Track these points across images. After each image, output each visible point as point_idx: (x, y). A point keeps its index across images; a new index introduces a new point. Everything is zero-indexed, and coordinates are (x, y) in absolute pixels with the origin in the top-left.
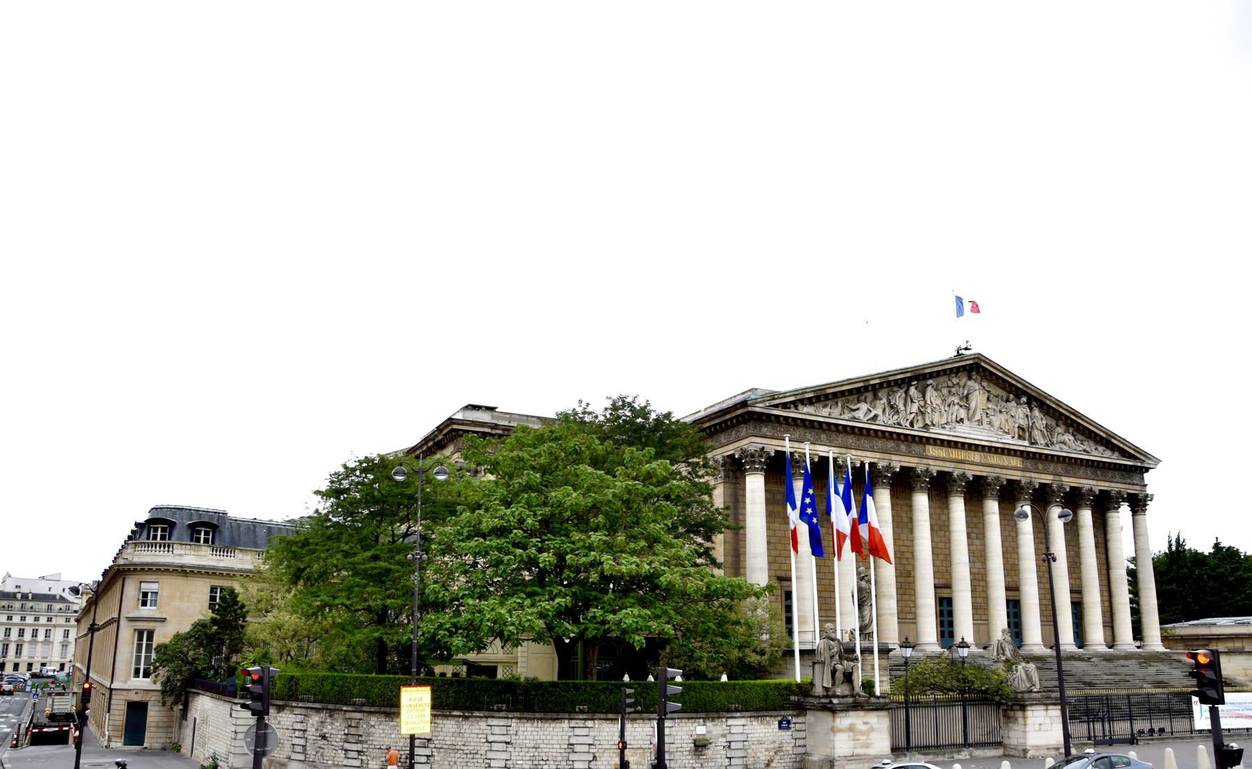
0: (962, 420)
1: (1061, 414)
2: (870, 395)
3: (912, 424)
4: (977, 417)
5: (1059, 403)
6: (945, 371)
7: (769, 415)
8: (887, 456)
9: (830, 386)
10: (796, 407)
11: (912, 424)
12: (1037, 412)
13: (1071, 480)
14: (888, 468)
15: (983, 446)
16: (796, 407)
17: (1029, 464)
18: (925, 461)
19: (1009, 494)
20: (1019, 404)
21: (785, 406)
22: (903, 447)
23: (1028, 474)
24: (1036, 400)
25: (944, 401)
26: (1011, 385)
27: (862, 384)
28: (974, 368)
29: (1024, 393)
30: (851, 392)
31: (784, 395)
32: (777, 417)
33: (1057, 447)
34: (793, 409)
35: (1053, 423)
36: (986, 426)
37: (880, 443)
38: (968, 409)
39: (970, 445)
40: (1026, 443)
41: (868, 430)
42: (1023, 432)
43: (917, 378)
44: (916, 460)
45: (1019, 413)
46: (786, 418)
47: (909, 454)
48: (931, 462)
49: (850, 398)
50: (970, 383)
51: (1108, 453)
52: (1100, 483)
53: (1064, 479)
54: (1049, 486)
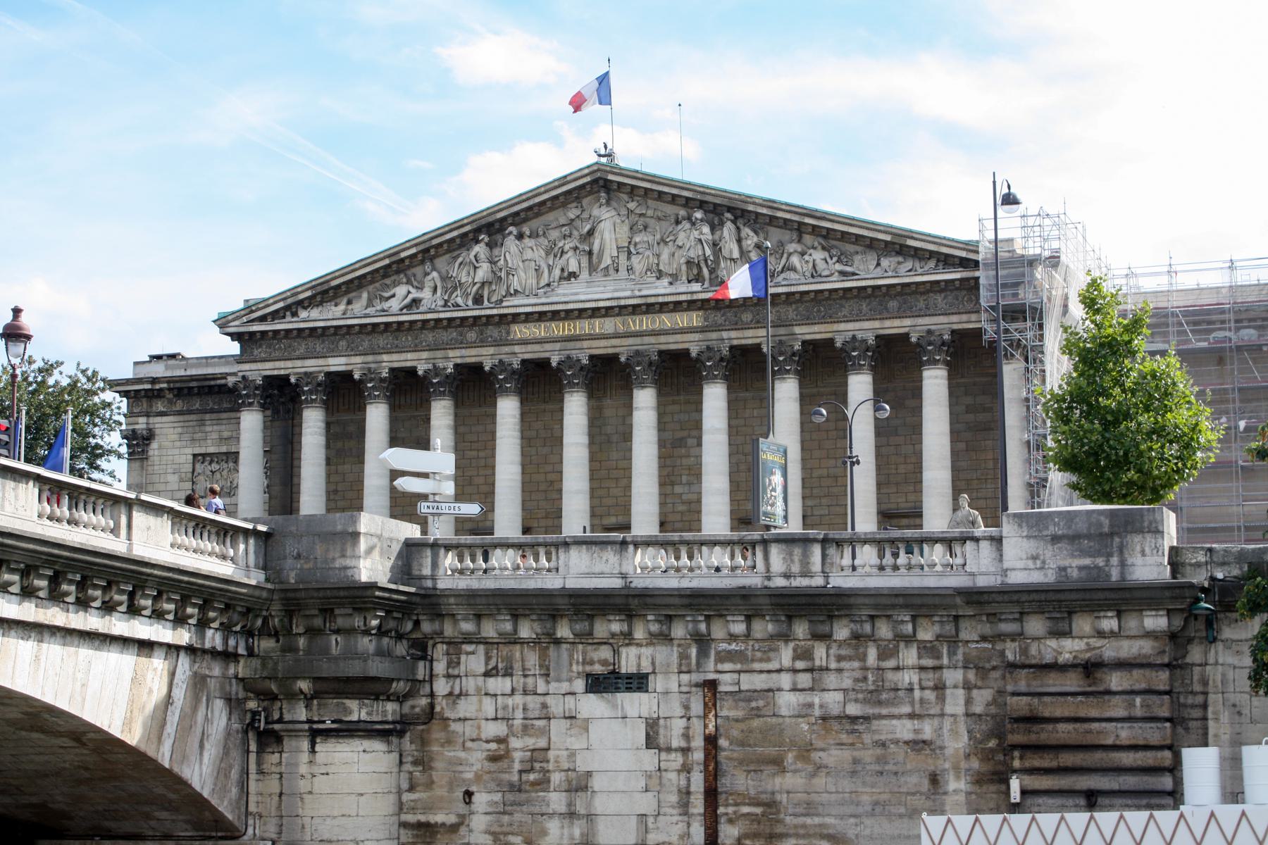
0: (573, 275)
1: (785, 220)
2: (418, 271)
3: (478, 300)
4: (607, 261)
5: (771, 204)
6: (543, 203)
7: (252, 334)
8: (439, 354)
9: (334, 275)
10: (295, 314)
11: (478, 300)
12: (728, 230)
13: (816, 328)
14: (436, 371)
15: (608, 309)
16: (295, 314)
17: (718, 317)
18: (507, 349)
19: (677, 374)
20: (693, 224)
21: (275, 315)
22: (472, 335)
23: (714, 335)
24: (730, 209)
25: (548, 254)
26: (674, 196)
27: (387, 261)
28: (602, 184)
29: (702, 205)
30: (385, 272)
31: (264, 302)
32: (264, 333)
33: (783, 276)
34: (289, 318)
35: (786, 235)
36: (623, 273)
37: (429, 337)
38: (590, 253)
39: (581, 311)
40: (696, 287)
41: (400, 323)
42: (695, 270)
43: (490, 228)
44: (491, 350)
45: (693, 238)
46: (276, 332)
47: (482, 343)
48: (517, 349)
49: (388, 281)
50: (596, 212)
51: (909, 265)
52: (888, 323)
53: (797, 330)
54: (759, 345)
